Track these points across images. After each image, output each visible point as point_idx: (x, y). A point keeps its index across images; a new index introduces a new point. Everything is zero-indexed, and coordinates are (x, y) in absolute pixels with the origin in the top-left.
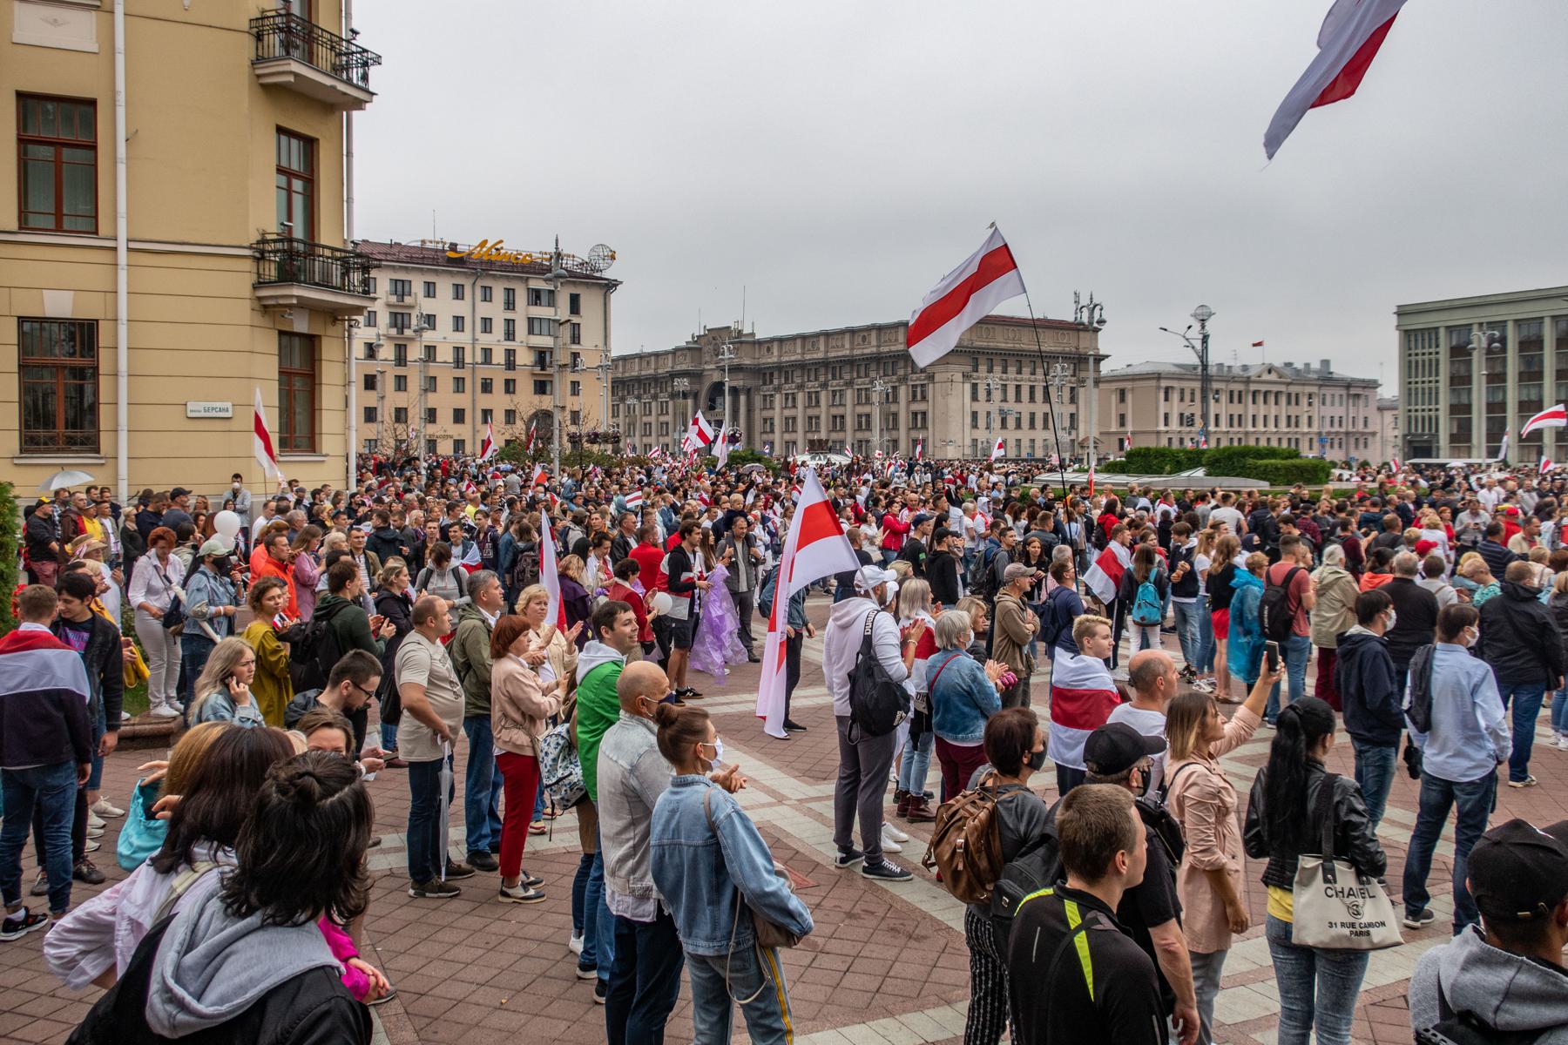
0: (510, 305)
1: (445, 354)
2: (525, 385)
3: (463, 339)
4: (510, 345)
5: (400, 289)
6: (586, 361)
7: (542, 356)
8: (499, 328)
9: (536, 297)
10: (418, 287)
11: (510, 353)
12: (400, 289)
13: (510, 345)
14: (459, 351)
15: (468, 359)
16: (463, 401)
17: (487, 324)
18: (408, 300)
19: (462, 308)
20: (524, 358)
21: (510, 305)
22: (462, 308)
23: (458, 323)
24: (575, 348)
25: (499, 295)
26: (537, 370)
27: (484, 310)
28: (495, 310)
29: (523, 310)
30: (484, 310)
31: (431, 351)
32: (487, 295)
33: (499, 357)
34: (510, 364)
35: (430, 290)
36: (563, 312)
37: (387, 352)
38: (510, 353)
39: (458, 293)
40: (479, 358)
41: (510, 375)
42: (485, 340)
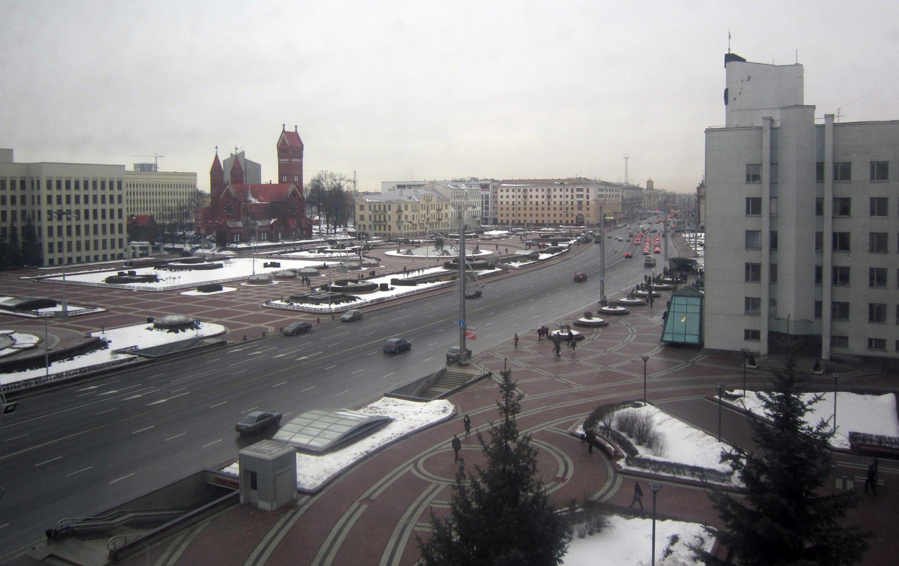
0: (572, 191)
1: (558, 203)
2: (576, 209)
3: (562, 200)
4: (572, 200)
5: (549, 190)
6: (590, 203)
7: (580, 203)
8: (570, 197)
9: (578, 190)
10: (552, 190)
11: (572, 202)
12: (549, 190)
13: (572, 200)
14: (561, 203)
15: (563, 204)
16: (561, 212)
17: (567, 196)
18: (550, 192)
19: (561, 193)
20: (576, 203)
21: (572, 191)
22: (561, 193)
23: (561, 196)
24: (588, 200)
25: (570, 190)
26: (578, 205)
27: (567, 193)
28: (569, 193)
29: (576, 193)
30: (567, 193)
31: (555, 202)
32: (567, 190)
33: (570, 203)
34: (572, 203)
35: (555, 190)
36: (585, 193)
37: (546, 203)
38: (572, 202)
39: (561, 190)
40: (565, 203)
41: (572, 206)
42: (567, 199)
